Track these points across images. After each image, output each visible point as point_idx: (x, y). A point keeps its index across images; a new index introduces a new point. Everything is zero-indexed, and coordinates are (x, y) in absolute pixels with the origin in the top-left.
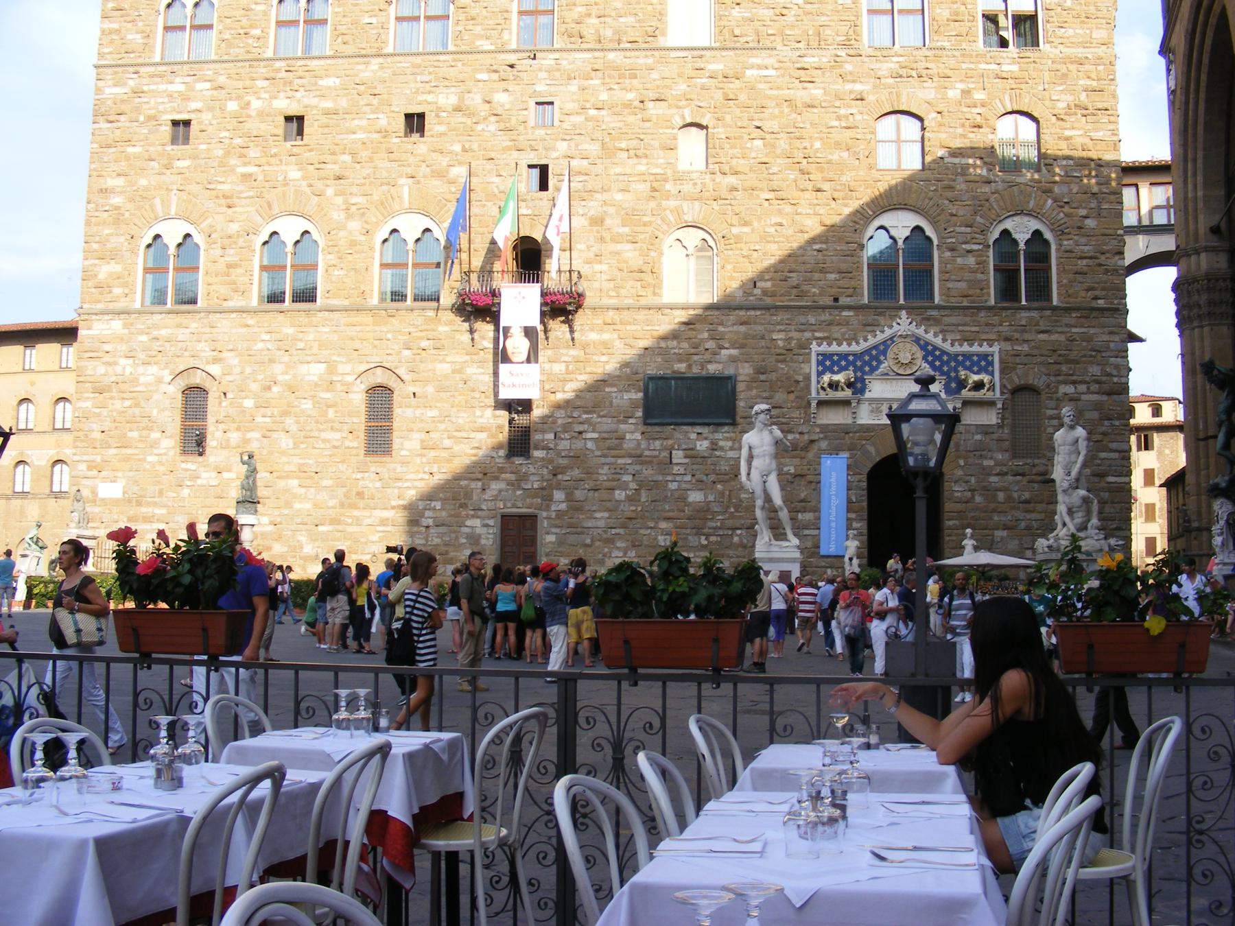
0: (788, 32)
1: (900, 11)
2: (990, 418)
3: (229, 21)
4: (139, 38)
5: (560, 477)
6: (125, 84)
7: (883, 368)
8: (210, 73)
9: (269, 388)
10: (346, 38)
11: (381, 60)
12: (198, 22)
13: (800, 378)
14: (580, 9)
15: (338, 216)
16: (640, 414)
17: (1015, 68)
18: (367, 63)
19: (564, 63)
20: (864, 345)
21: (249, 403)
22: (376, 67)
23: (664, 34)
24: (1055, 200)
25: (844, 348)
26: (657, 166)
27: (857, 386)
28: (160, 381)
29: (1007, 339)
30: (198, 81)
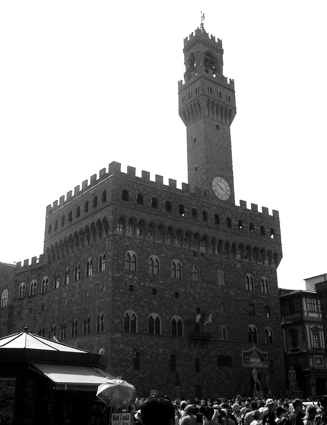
2: (267, 366)
5: (205, 377)
6: (119, 274)
7: (252, 356)
9: (153, 354)
13: (240, 357)
15: (164, 314)
16: (217, 364)
17: (266, 297)
20: (249, 351)
21: (148, 357)
22: (169, 280)
24: (273, 324)
25: (247, 351)
26: (218, 311)
27: (249, 359)
28: (130, 350)
29: (268, 351)
30: (135, 276)
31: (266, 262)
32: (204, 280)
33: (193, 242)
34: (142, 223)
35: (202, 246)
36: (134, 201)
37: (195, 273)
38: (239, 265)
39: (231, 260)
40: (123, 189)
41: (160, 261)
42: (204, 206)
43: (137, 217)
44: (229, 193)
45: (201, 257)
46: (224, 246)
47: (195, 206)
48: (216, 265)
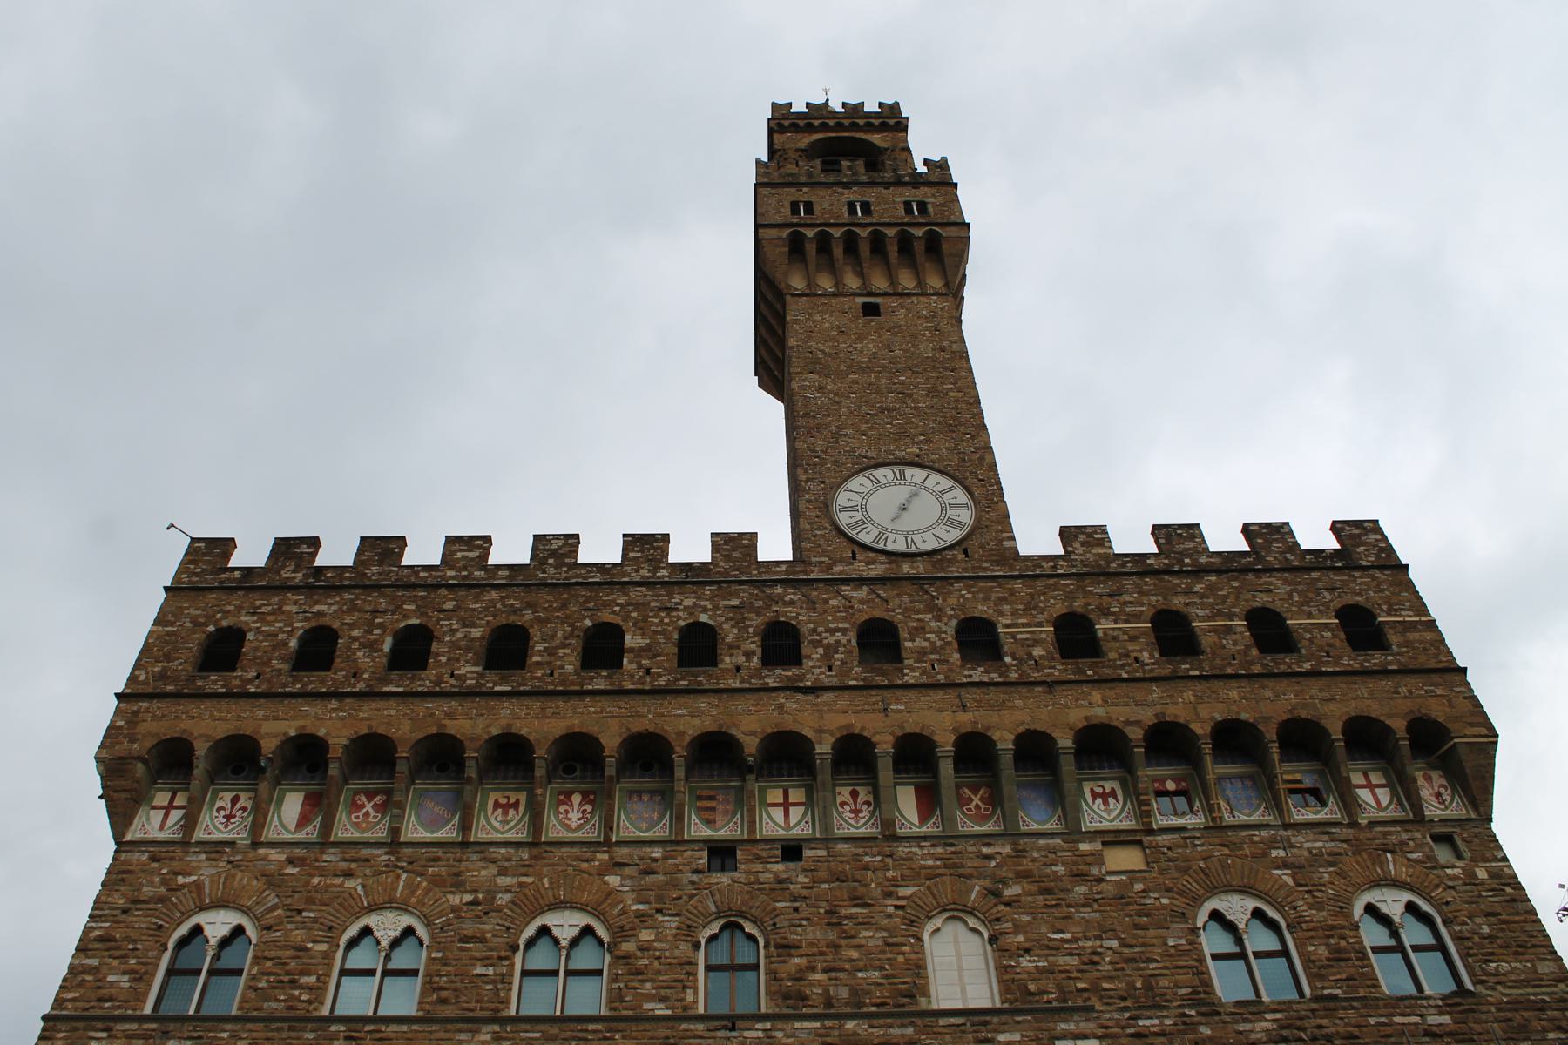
0: (1106, 985)
1: (1257, 955)
3: (269, 964)
4: (125, 981)
8: (225, 1035)
10: (444, 994)
11: (496, 1028)
12: (221, 965)
14: (797, 960)
18: (477, 1031)
19: (779, 1034)
22: (488, 1037)
23: (925, 993)
31: (1374, 797)
32: (803, 998)
33: (711, 798)
34: (306, 756)
35: (786, 805)
36: (267, 663)
37: (733, 968)
38: (1126, 859)
39: (1042, 842)
40: (211, 628)
41: (432, 936)
42: (778, 600)
43: (268, 727)
44: (967, 517)
45: (780, 867)
46: (946, 769)
47: (705, 610)
48: (903, 892)
